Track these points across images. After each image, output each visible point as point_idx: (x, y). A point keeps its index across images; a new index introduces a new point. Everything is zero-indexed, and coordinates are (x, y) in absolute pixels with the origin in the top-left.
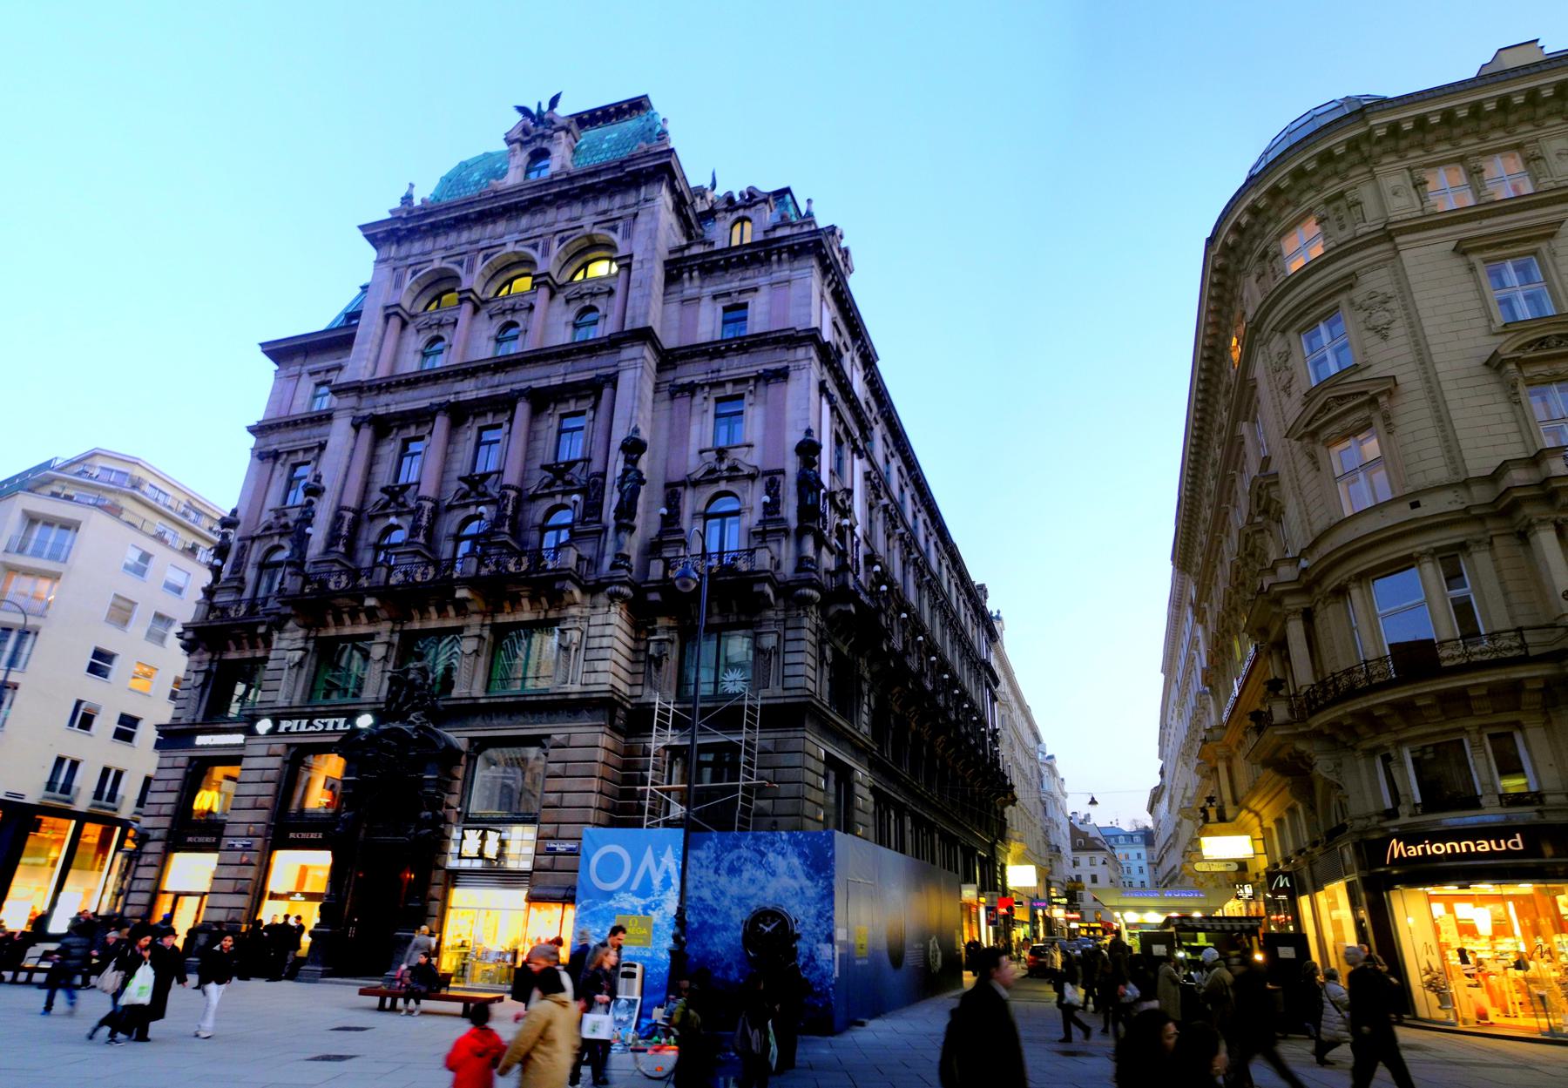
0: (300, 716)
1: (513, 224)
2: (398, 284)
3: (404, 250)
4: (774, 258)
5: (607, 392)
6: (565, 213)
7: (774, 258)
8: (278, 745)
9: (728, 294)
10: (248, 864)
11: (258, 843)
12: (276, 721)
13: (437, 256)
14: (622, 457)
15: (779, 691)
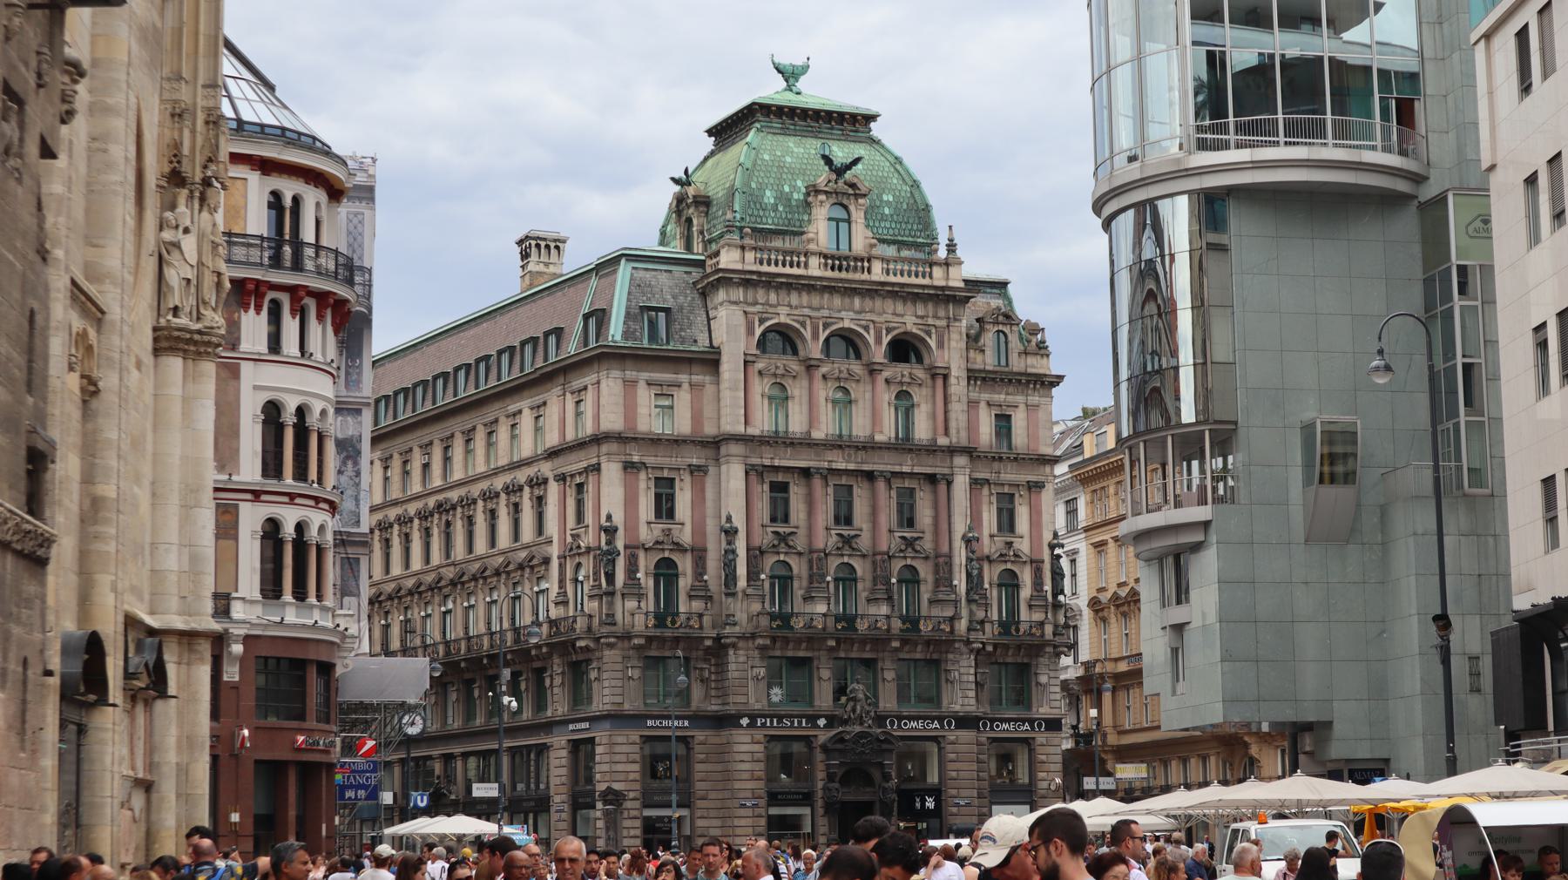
0: (772, 717)
1: (847, 300)
2: (750, 331)
3: (750, 293)
5: (942, 487)
6: (889, 305)
8: (759, 735)
10: (760, 816)
11: (763, 802)
12: (753, 718)
13: (783, 310)
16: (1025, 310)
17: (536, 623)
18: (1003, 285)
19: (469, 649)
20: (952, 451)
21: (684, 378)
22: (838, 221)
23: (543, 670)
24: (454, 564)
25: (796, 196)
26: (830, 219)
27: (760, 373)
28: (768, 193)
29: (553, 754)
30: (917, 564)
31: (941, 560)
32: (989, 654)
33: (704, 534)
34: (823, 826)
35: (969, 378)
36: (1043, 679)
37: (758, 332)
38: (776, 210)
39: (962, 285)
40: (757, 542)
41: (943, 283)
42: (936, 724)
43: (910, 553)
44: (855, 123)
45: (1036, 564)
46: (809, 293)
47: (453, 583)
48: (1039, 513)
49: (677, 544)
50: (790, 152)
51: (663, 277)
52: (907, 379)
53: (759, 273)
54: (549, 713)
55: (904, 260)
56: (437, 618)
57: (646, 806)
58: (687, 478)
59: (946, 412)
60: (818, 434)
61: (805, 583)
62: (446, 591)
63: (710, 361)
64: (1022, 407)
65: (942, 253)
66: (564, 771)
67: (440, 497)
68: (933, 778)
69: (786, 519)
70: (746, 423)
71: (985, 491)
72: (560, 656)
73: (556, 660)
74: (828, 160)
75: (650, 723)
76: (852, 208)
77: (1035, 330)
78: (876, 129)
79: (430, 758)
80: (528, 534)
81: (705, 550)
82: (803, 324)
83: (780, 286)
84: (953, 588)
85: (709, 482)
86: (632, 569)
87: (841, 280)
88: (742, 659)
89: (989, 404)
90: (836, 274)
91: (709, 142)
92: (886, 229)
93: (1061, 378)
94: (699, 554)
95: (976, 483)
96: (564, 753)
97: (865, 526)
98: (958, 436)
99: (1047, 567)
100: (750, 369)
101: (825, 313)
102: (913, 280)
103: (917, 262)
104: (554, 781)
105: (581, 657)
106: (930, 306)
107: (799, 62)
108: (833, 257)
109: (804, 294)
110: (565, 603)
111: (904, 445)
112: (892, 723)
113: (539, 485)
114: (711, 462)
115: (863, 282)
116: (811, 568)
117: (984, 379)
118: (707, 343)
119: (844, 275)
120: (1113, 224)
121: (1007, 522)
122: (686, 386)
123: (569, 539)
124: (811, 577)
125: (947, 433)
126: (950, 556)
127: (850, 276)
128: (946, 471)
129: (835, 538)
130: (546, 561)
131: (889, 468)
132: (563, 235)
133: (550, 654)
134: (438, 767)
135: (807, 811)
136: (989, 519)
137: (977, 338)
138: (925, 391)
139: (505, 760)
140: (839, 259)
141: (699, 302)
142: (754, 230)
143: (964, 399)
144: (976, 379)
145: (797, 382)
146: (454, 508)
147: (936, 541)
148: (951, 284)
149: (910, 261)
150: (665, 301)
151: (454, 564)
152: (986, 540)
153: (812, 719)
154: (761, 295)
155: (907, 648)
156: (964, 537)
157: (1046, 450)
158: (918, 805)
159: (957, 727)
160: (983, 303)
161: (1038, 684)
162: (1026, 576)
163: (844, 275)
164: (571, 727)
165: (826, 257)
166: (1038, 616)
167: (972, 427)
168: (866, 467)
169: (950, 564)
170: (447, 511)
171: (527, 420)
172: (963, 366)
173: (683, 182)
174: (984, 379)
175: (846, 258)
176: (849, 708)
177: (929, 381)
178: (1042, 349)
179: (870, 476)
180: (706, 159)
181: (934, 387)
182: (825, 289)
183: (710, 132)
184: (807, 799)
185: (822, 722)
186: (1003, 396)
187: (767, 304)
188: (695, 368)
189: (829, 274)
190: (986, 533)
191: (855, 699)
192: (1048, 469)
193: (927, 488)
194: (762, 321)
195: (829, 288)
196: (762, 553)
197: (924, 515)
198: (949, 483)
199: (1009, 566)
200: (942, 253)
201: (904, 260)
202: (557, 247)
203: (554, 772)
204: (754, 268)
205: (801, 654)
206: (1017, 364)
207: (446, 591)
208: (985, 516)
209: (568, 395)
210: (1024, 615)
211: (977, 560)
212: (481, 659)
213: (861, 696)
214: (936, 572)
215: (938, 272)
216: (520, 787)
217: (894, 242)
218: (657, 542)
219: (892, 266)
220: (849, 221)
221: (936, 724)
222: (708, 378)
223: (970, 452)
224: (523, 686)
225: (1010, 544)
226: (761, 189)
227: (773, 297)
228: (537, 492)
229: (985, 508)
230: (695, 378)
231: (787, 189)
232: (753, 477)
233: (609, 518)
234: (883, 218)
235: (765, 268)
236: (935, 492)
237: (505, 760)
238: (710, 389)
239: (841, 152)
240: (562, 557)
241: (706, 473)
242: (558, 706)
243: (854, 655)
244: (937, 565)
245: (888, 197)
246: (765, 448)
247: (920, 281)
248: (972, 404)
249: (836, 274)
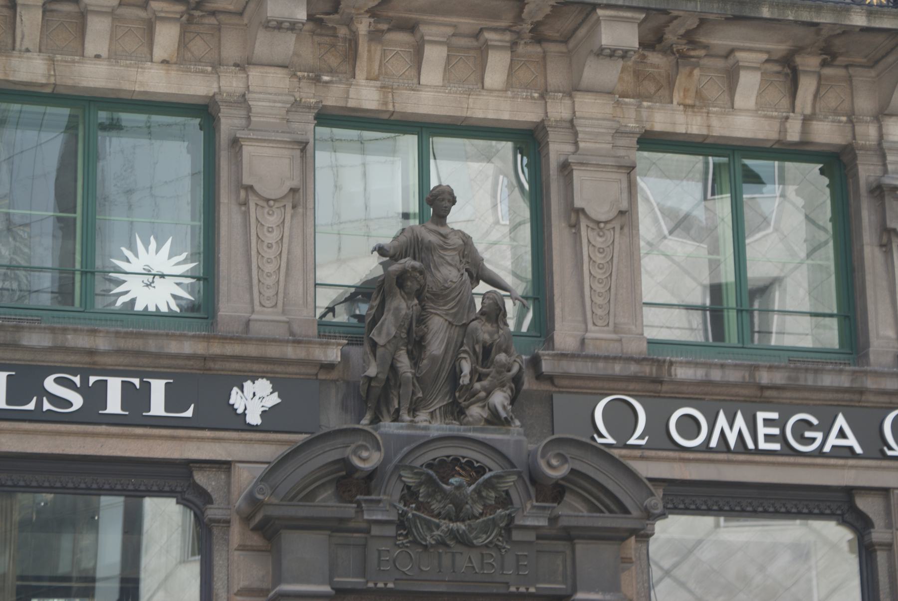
42: (842, 433)
112: (620, 419)
185: (254, 399)
205: (155, 80)
221: (842, 433)
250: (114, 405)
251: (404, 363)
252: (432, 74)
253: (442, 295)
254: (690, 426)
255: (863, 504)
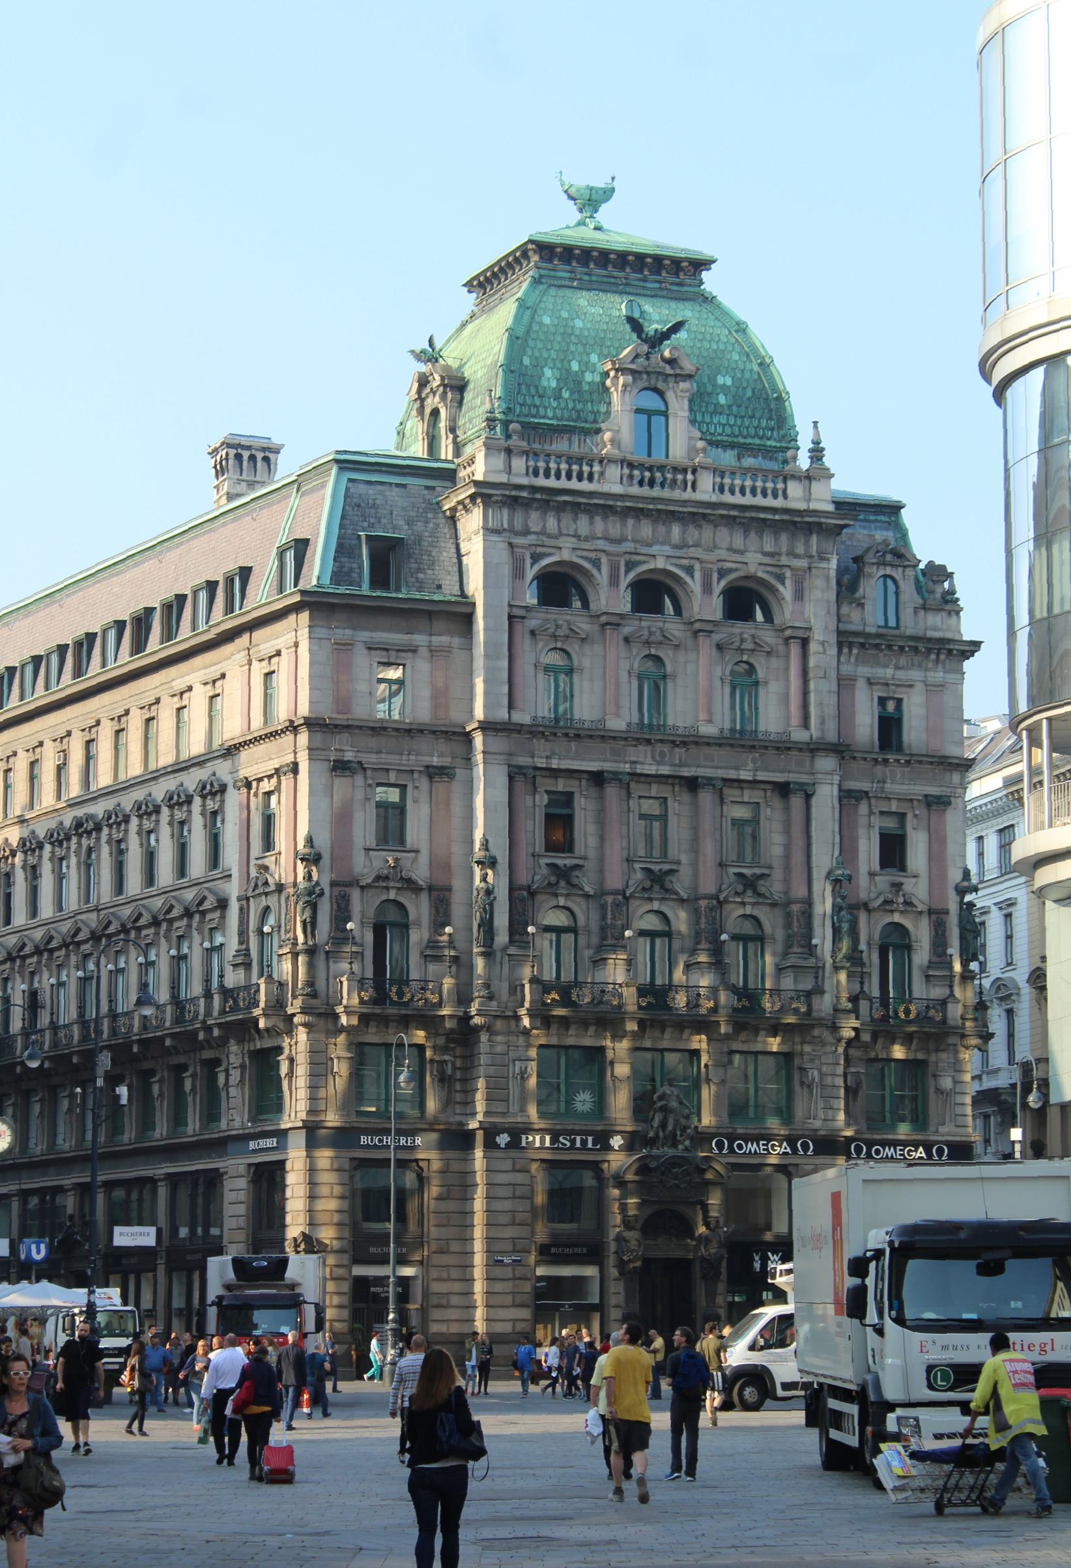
1: (661, 529)
4: (933, 657)
5: (797, 801)
6: (723, 536)
7: (933, 657)
9: (887, 684)
13: (567, 543)
14: (829, 888)
15: (954, 1129)
16: (925, 548)
17: (208, 995)
18: (894, 509)
19: (114, 1032)
20: (814, 749)
21: (420, 639)
22: (649, 413)
23: (216, 1062)
24: (97, 909)
25: (588, 377)
26: (638, 411)
27: (533, 633)
28: (548, 372)
29: (228, 1184)
30: (762, 913)
31: (795, 908)
32: (866, 1046)
33: (447, 868)
34: (617, 1294)
35: (840, 645)
36: (946, 1083)
37: (530, 573)
38: (558, 397)
39: (830, 508)
40: (523, 878)
41: (802, 506)
43: (749, 897)
44: (678, 273)
45: (937, 916)
46: (605, 518)
47: (95, 937)
48: (943, 841)
49: (409, 881)
50: (576, 313)
51: (394, 495)
52: (748, 645)
53: (534, 489)
54: (223, 1125)
55: (745, 471)
56: (73, 987)
57: (358, 1260)
58: (424, 783)
59: (805, 693)
60: (617, 724)
61: (595, 940)
62: (86, 948)
63: (460, 616)
64: (920, 687)
65: (804, 462)
66: (242, 1209)
67: (80, 812)
68: (780, 1227)
69: (567, 846)
70: (511, 706)
71: (863, 808)
72: (241, 1041)
73: (234, 1047)
74: (636, 325)
75: (364, 1140)
76: (670, 395)
77: (937, 573)
78: (710, 281)
79: (60, 1190)
80: (197, 864)
81: (449, 889)
82: (597, 564)
83: (561, 508)
84: (811, 950)
85: (457, 788)
86: (341, 914)
87: (654, 500)
88: (499, 1049)
89: (870, 682)
90: (645, 491)
91: (469, 300)
92: (720, 425)
93: (976, 645)
94: (440, 897)
95: (848, 798)
96: (242, 1183)
97: (684, 858)
98: (822, 726)
99: (953, 920)
100: (518, 627)
101: (628, 546)
102: (759, 501)
103: (765, 473)
104: (229, 1223)
105: (268, 1043)
106: (784, 537)
107: (600, 183)
108: (641, 466)
109: (598, 520)
110: (248, 966)
111: (742, 740)
112: (720, 1145)
113: (213, 794)
114: (459, 762)
115: (685, 503)
116: (603, 917)
117: (862, 645)
118: (456, 590)
119: (656, 492)
120: (1009, 393)
121: (893, 851)
122: (424, 651)
123: (253, 873)
124: (603, 930)
125: (806, 724)
126: (808, 902)
127: (666, 493)
128: (804, 778)
129: (639, 875)
130: (223, 904)
131: (721, 773)
132: (276, 440)
133: (223, 1042)
134: (70, 1203)
135: (590, 1271)
136: (868, 850)
137: (853, 586)
138: (774, 662)
139: (163, 1192)
140: (650, 469)
141: (446, 530)
142: (525, 425)
143: (833, 675)
144: (851, 645)
145: (587, 648)
146: (98, 828)
147: (787, 881)
148: (814, 506)
149: (754, 472)
150: (395, 528)
151: (97, 909)
152: (863, 880)
153: (603, 1140)
154: (534, 519)
155: (743, 1036)
156: (828, 876)
157: (952, 751)
158: (757, 1266)
159: (816, 1152)
160: (861, 535)
161: (939, 1091)
162: (922, 934)
163: (656, 492)
164: (252, 1145)
165: (631, 466)
166: (938, 992)
167: (844, 713)
168: (686, 772)
169: (808, 915)
170: (89, 833)
171: (198, 701)
172: (833, 625)
173: (430, 355)
174: (862, 645)
175: (662, 468)
176: (656, 1123)
177: (781, 648)
178: (949, 604)
179: (692, 785)
180: (464, 325)
181: (787, 657)
182: (626, 513)
183: (469, 285)
184: (594, 1255)
186: (889, 672)
187: (544, 532)
188: (439, 625)
189: (635, 490)
190: (863, 869)
191: (665, 1109)
192: (956, 777)
193: (777, 803)
194: (536, 558)
195: (636, 511)
196: (532, 894)
197: (774, 843)
198: (808, 797)
199: (897, 918)
200: (804, 462)
201: (745, 471)
202: (266, 459)
203: (229, 1210)
204: (525, 481)
206: (911, 624)
207: (86, 948)
208: (863, 845)
209: (256, 665)
210: (919, 989)
211: (849, 909)
212: (129, 1045)
213: (674, 1104)
214: (788, 925)
215: (795, 489)
216: (184, 1232)
217: (732, 446)
218: (378, 878)
219: (727, 481)
220: (665, 414)
222: (456, 641)
223: (841, 750)
224: (188, 1085)
225: (897, 886)
226: (537, 365)
227: (552, 523)
228: (211, 805)
229: (862, 832)
230: (437, 640)
231: (575, 366)
232: (520, 785)
233: (310, 841)
234: (718, 410)
235: (541, 482)
236: (787, 809)
237: (163, 1192)
238: (459, 656)
239: (657, 315)
240: (245, 899)
241: (452, 777)
242: (235, 1115)
243: (665, 1044)
244: (788, 915)
245: (724, 380)
246: (539, 745)
247: (769, 502)
248: (844, 684)
249: (645, 491)
250: (578, 1145)
251: (661, 1134)
252: (667, 1035)
253: (672, 1111)
254: (740, 1147)
255: (790, 1168)
